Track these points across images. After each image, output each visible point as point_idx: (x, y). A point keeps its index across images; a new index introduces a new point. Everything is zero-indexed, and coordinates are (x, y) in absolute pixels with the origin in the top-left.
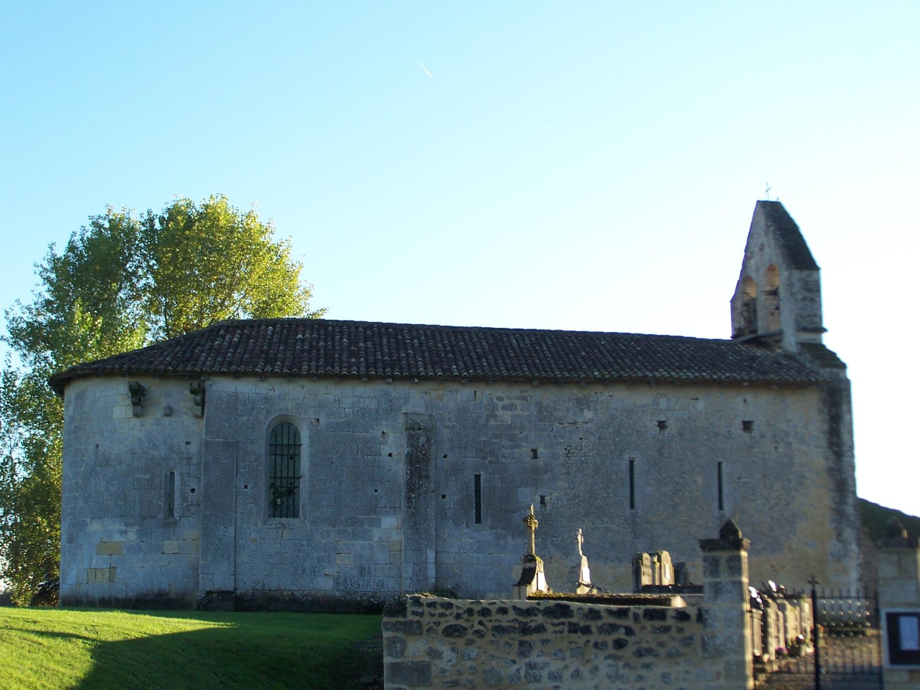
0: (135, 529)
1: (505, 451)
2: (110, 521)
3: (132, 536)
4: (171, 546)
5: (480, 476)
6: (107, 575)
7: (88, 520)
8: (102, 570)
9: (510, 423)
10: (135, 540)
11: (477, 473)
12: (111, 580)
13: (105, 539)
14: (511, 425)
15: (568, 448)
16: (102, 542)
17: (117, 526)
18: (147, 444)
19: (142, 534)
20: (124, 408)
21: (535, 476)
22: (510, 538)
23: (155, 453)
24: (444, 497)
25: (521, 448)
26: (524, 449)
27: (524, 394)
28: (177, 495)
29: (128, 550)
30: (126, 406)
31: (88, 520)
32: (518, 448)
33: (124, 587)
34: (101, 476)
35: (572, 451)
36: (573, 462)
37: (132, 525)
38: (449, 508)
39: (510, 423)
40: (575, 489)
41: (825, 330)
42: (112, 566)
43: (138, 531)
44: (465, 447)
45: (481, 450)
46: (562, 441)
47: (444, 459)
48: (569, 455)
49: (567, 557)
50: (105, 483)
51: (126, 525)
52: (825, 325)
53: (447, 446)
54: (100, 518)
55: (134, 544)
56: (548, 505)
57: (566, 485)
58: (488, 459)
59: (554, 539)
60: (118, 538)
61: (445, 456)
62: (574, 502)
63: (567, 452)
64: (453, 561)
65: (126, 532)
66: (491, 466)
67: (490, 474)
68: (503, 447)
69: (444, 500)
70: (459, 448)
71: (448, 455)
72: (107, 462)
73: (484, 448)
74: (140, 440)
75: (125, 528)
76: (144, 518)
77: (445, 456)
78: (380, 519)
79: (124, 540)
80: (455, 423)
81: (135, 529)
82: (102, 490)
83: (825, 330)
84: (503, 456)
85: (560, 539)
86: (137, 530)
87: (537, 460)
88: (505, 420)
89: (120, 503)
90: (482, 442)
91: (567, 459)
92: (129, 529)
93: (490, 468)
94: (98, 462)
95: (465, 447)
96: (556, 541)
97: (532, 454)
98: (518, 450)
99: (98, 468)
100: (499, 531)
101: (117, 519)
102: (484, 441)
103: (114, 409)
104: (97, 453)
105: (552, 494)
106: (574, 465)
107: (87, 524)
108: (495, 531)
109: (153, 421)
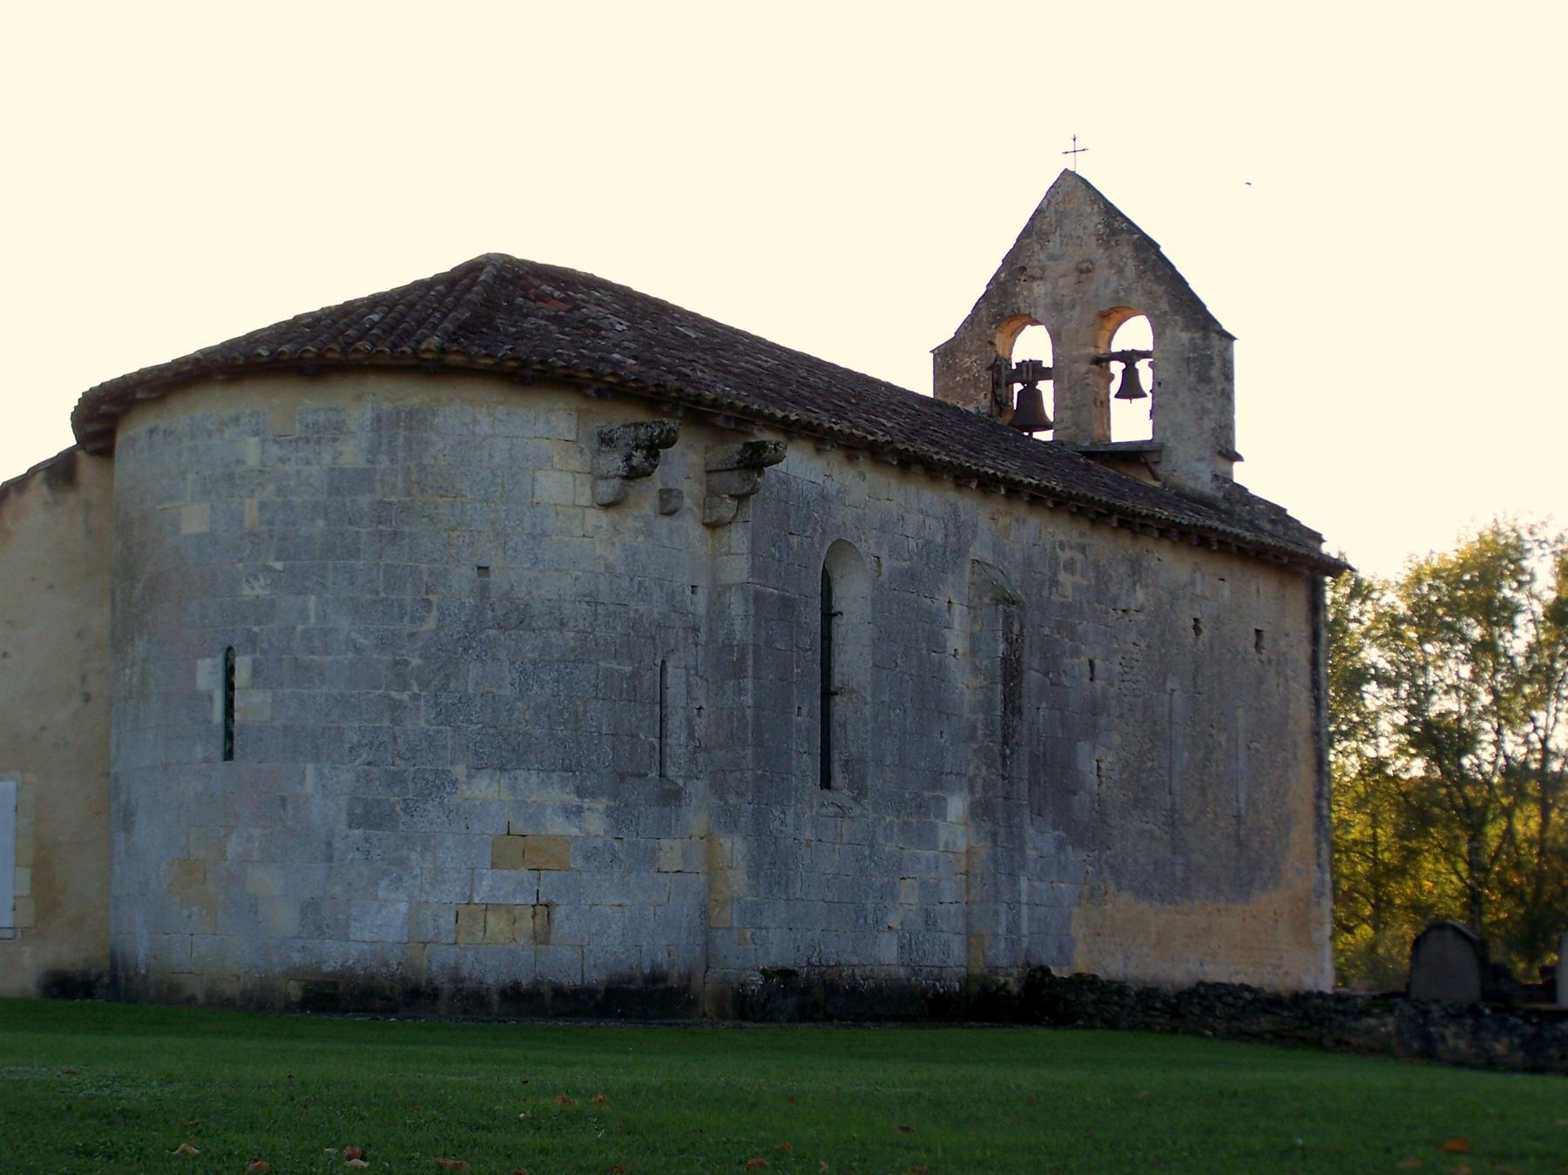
0: (601, 804)
2: (534, 778)
3: (596, 823)
4: (671, 852)
6: (527, 924)
7: (460, 771)
8: (509, 909)
9: (1070, 600)
10: (602, 833)
12: (542, 937)
13: (519, 827)
16: (508, 834)
17: (557, 794)
18: (625, 582)
19: (620, 817)
20: (569, 478)
22: (1070, 847)
23: (642, 608)
27: (1085, 540)
28: (675, 721)
29: (586, 859)
30: (573, 473)
31: (460, 771)
33: (578, 956)
34: (502, 654)
37: (593, 795)
41: (1239, 458)
42: (543, 900)
43: (610, 812)
50: (515, 675)
51: (581, 792)
52: (1239, 448)
54: (502, 769)
55: (599, 843)
60: (558, 826)
65: (580, 810)
72: (519, 618)
74: (609, 568)
75: (576, 801)
76: (622, 778)
78: (945, 799)
79: (574, 831)
81: (601, 804)
82: (507, 691)
83: (1239, 458)
86: (608, 808)
89: (561, 731)
92: (587, 803)
94: (490, 614)
99: (492, 632)
101: (555, 777)
103: (540, 476)
104: (484, 588)
107: (454, 783)
109: (639, 525)
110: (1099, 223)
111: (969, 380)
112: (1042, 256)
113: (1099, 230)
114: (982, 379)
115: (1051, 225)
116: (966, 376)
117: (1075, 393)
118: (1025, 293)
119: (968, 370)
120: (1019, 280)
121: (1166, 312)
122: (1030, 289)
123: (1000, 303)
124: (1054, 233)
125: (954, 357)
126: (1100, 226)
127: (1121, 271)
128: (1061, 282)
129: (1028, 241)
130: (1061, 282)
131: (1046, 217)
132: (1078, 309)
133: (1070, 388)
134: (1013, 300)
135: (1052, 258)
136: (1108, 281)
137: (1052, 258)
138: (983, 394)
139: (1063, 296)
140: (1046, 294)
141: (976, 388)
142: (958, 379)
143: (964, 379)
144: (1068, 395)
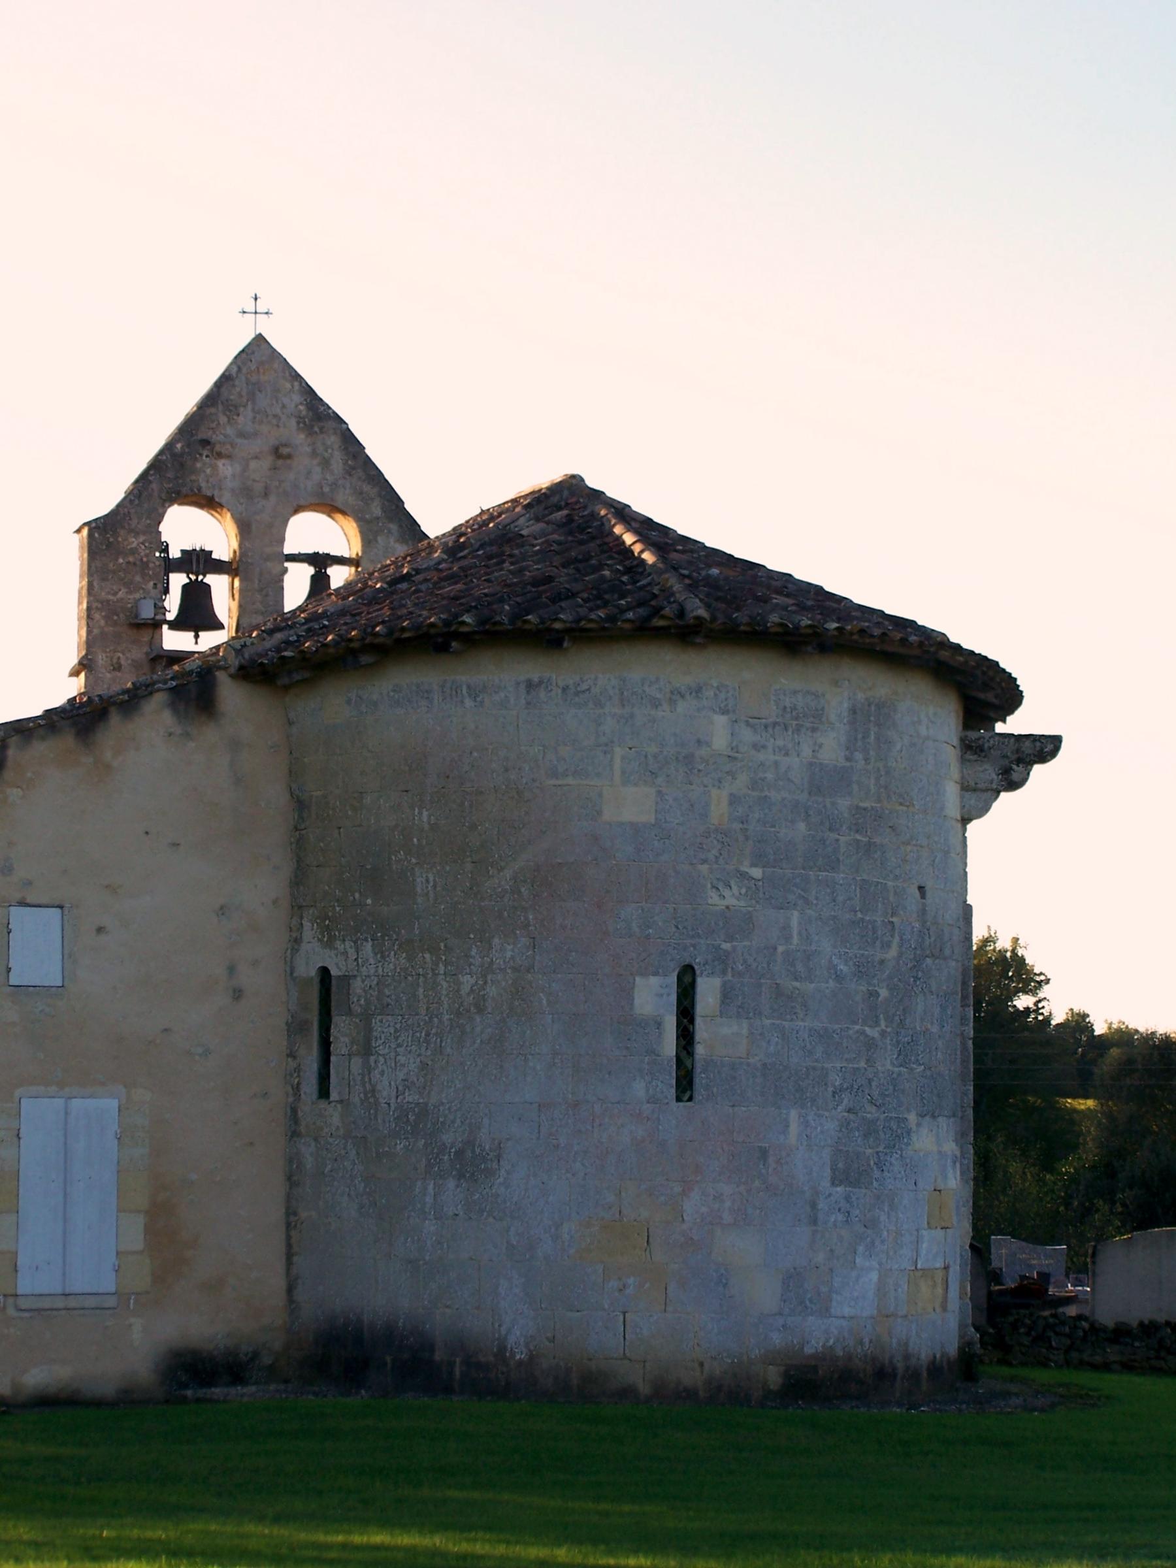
110: (301, 404)
111: (135, 564)
112: (229, 431)
113: (300, 411)
114: (151, 565)
115: (241, 396)
116: (131, 559)
117: (267, 595)
118: (208, 471)
119: (133, 552)
120: (201, 455)
121: (378, 518)
122: (214, 467)
123: (177, 478)
124: (245, 406)
125: (115, 534)
126: (301, 407)
127: (326, 463)
128: (253, 464)
129: (213, 410)
130: (253, 464)
131: (234, 386)
132: (273, 499)
133: (261, 590)
134: (193, 477)
135: (242, 435)
136: (309, 473)
137: (242, 435)
138: (152, 583)
139: (254, 481)
140: (234, 476)
141: (143, 575)
142: (121, 561)
143: (129, 563)
144: (258, 597)
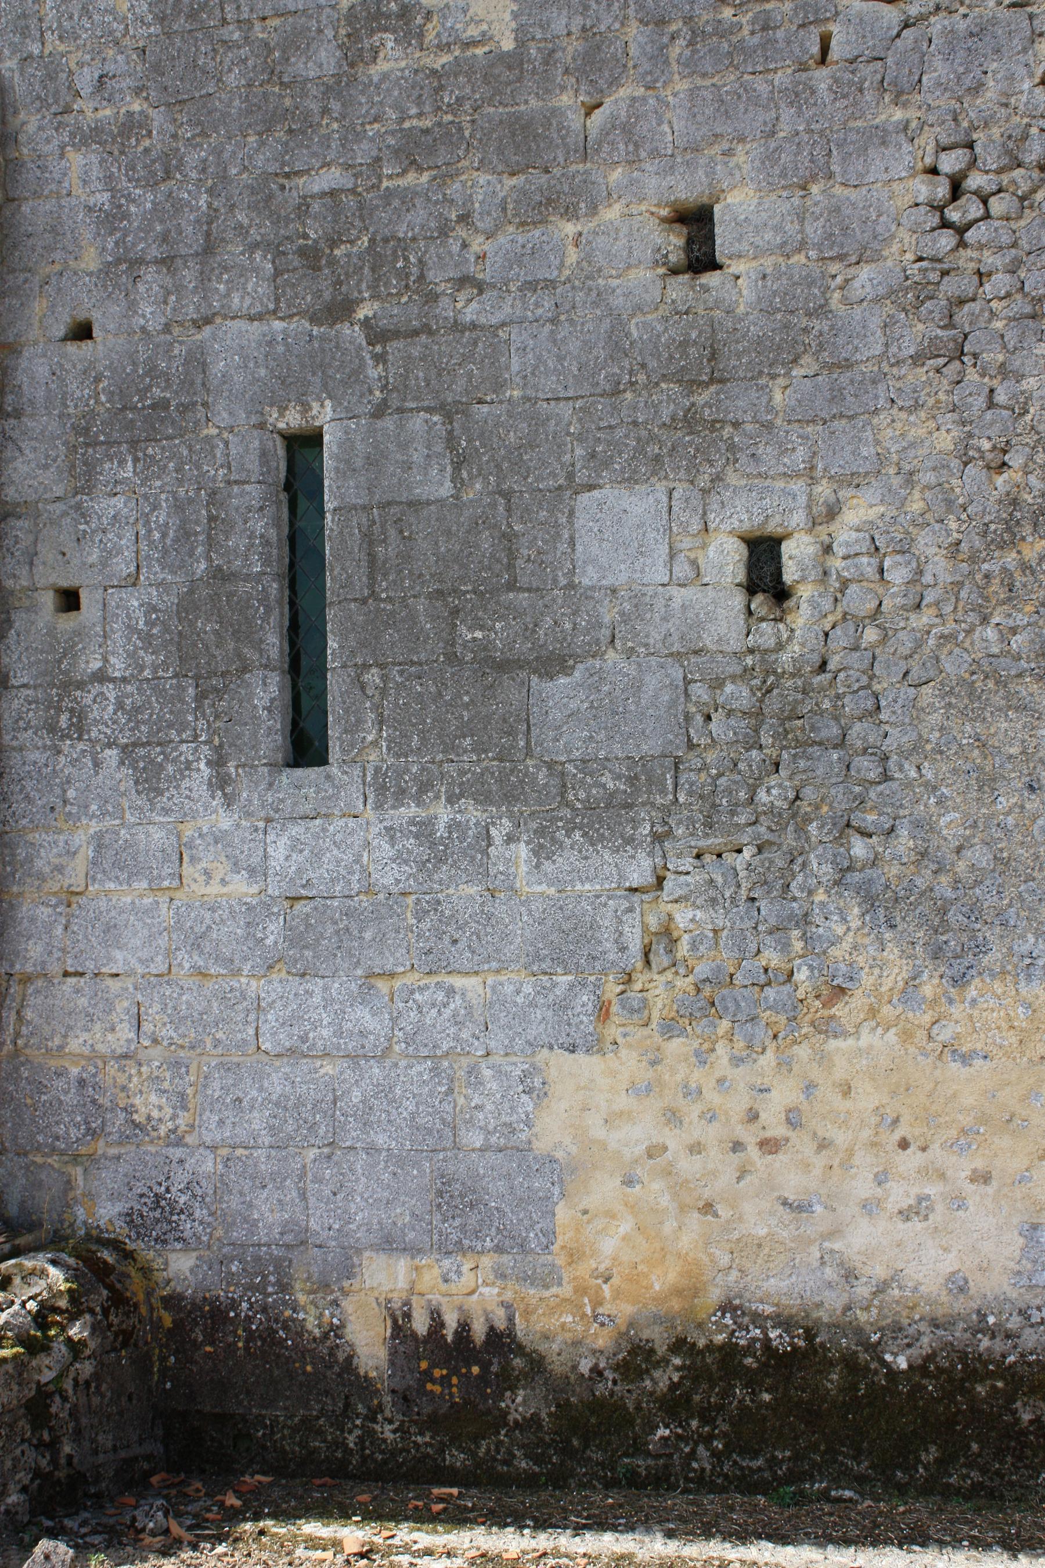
1: (477, 244)
5: (310, 440)
9: (508, 44)
11: (292, 420)
14: (515, 61)
15: (949, 163)
21: (702, 397)
22: (523, 850)
24: (70, 600)
25: (593, 210)
26: (611, 214)
32: (570, 213)
35: (975, 181)
36: (990, 260)
38: (101, 677)
39: (508, 44)
40: (1016, 459)
44: (209, 249)
45: (311, 257)
46: (898, 115)
47: (72, 348)
48: (954, 215)
49: (960, 981)
53: (91, 260)
56: (805, 592)
57: (946, 441)
58: (363, 312)
59: (859, 848)
61: (83, 332)
62: (1010, 559)
63: (943, 190)
64: (125, 1032)
66: (380, 359)
67: (379, 412)
68: (464, 218)
69: (67, 622)
70: (167, 262)
71: (96, 316)
73: (333, 244)
77: (83, 332)
80: (136, 107)
84: (463, 281)
85: (904, 842)
87: (712, 279)
88: (473, 32)
90: (316, 207)
91: (946, 240)
93: (373, 372)
95: (209, 249)
96: (875, 861)
97: (674, 242)
98: (570, 228)
100: (444, 814)
102: (332, 193)
105: (832, 513)
106: (1001, 282)
108: (410, 811)
